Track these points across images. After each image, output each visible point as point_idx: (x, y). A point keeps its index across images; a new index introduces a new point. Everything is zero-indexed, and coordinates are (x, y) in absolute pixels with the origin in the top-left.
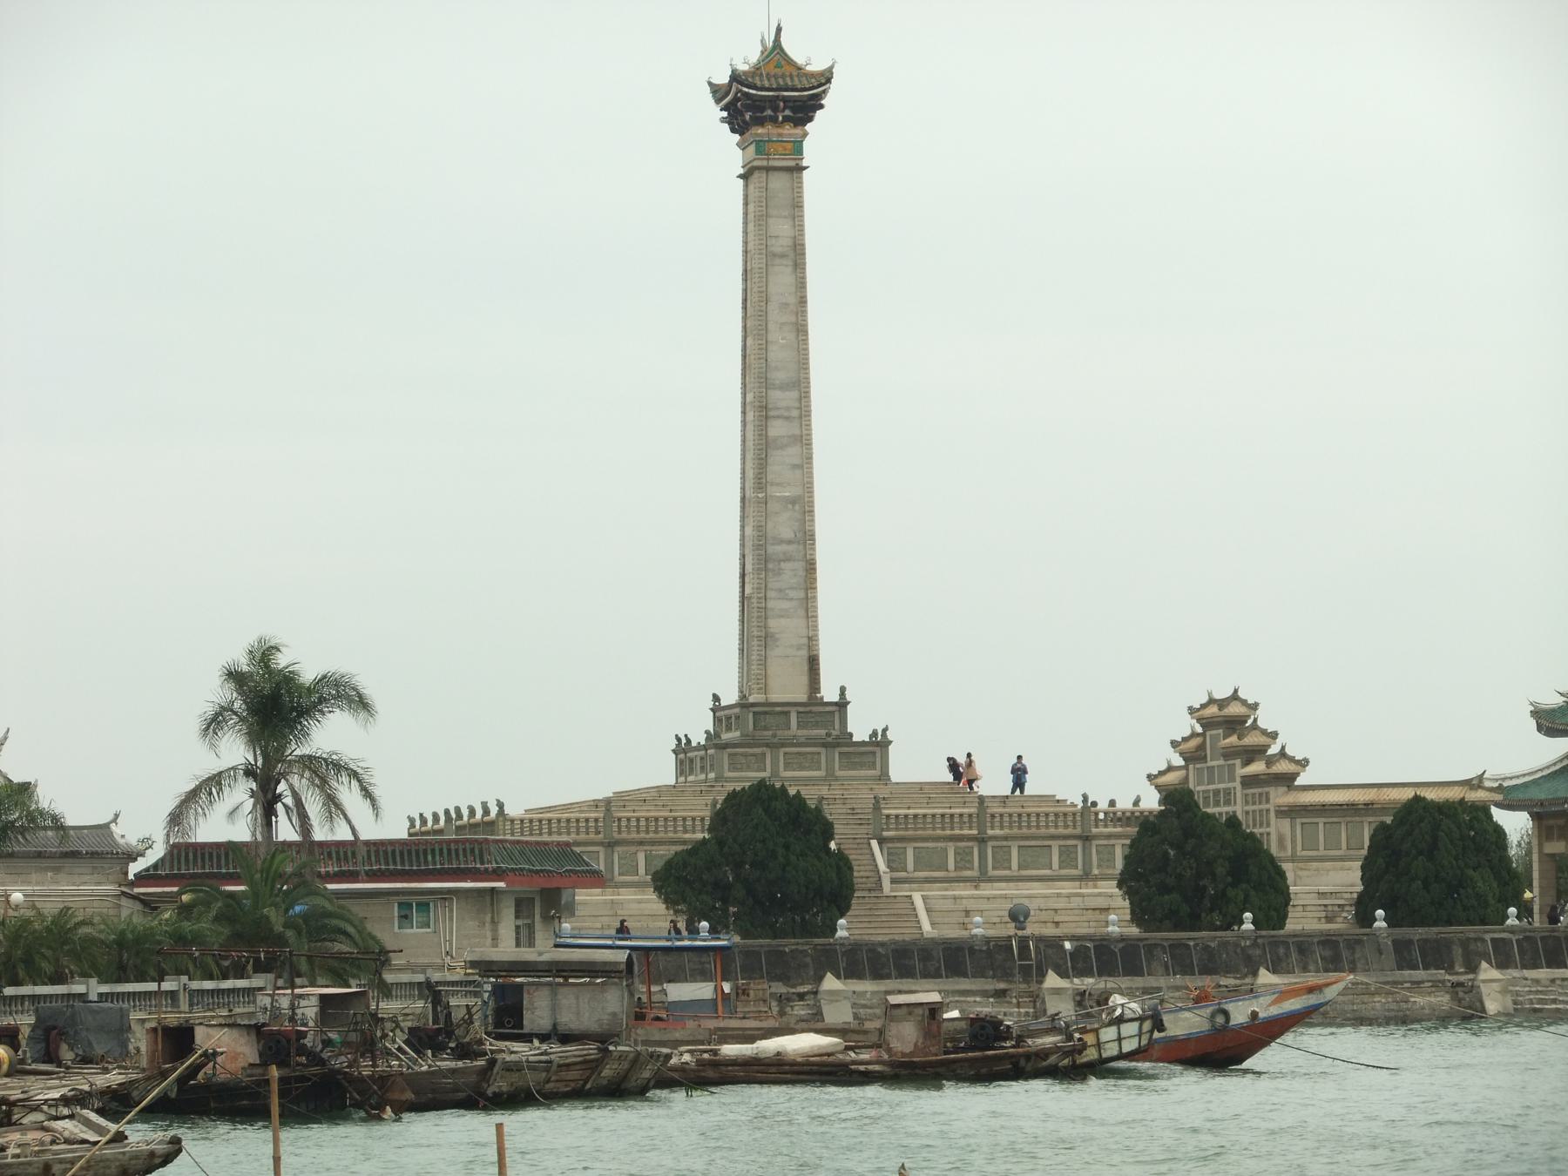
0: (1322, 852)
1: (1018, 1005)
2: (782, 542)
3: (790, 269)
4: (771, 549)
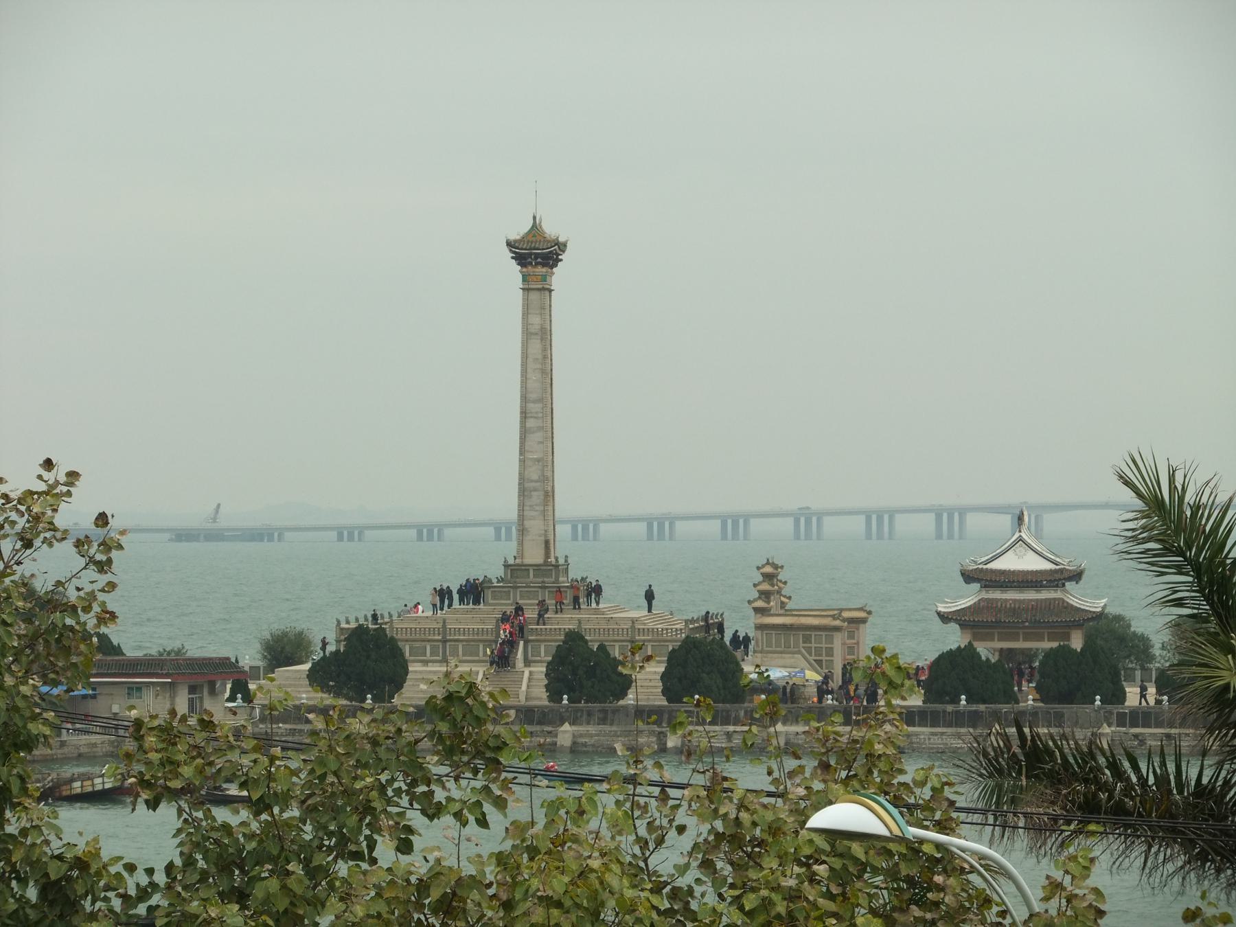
0: (774, 649)
4: (527, 485)
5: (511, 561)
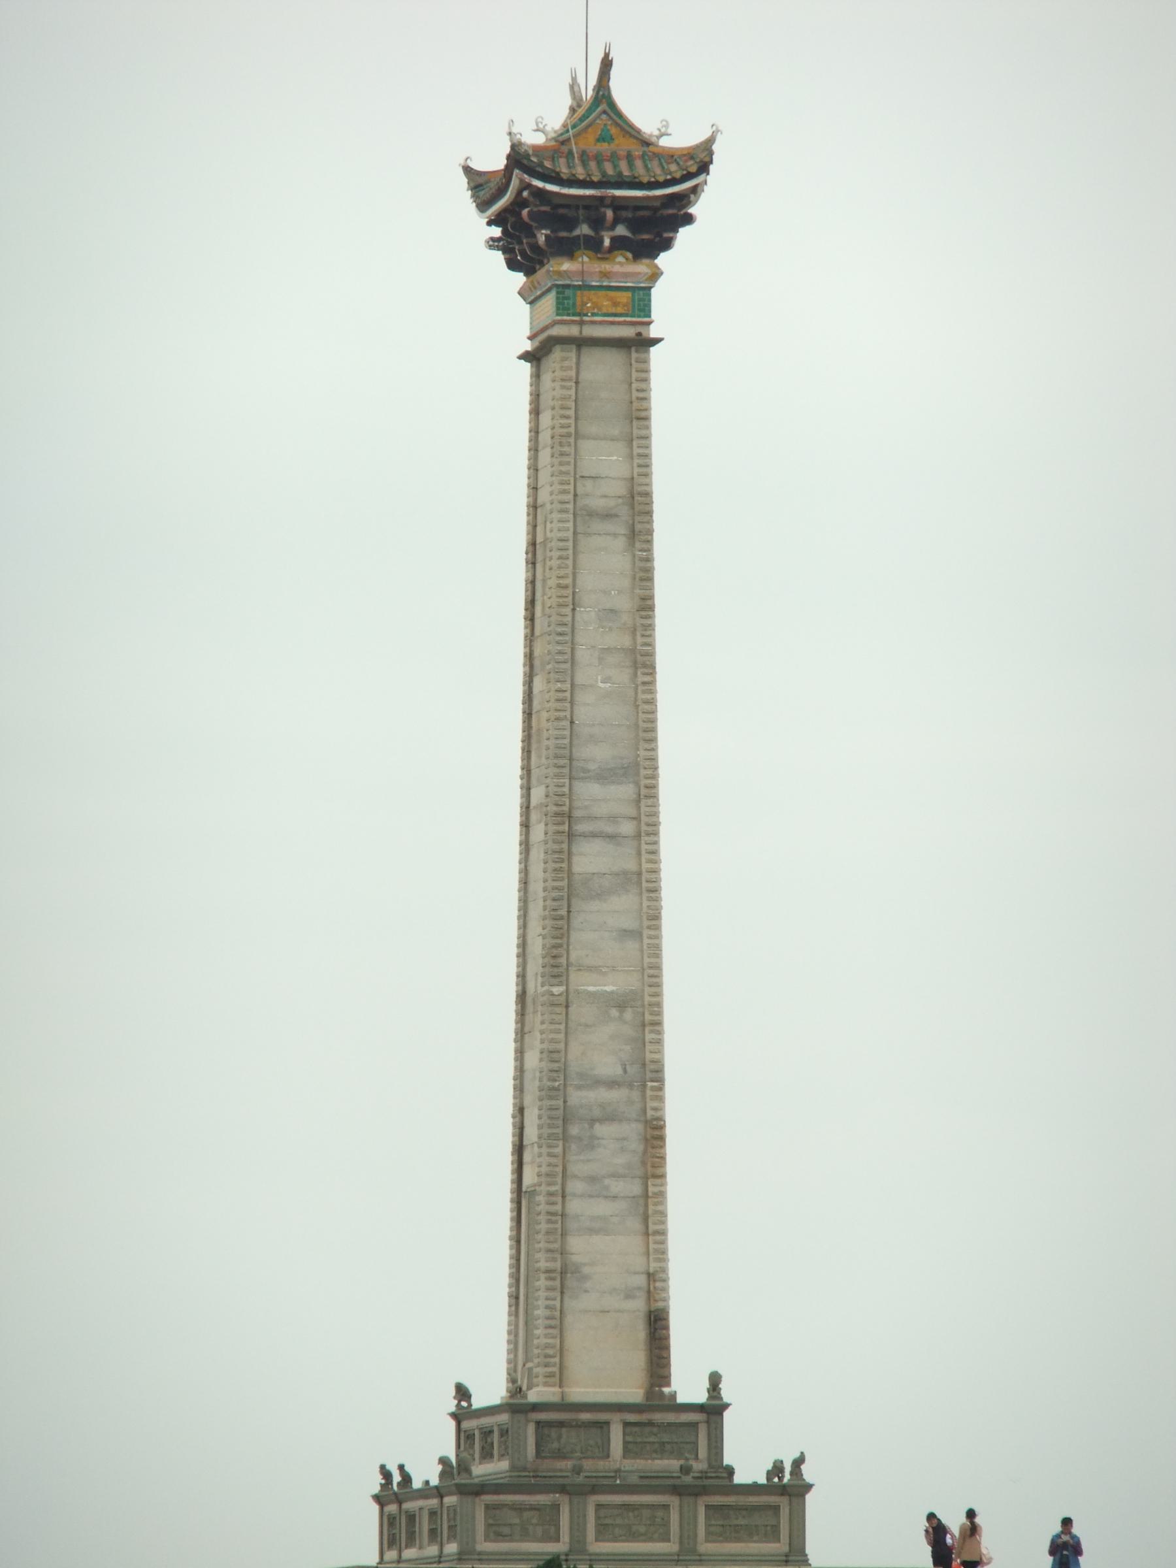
2: (598, 1082)
3: (620, 543)
4: (576, 1097)
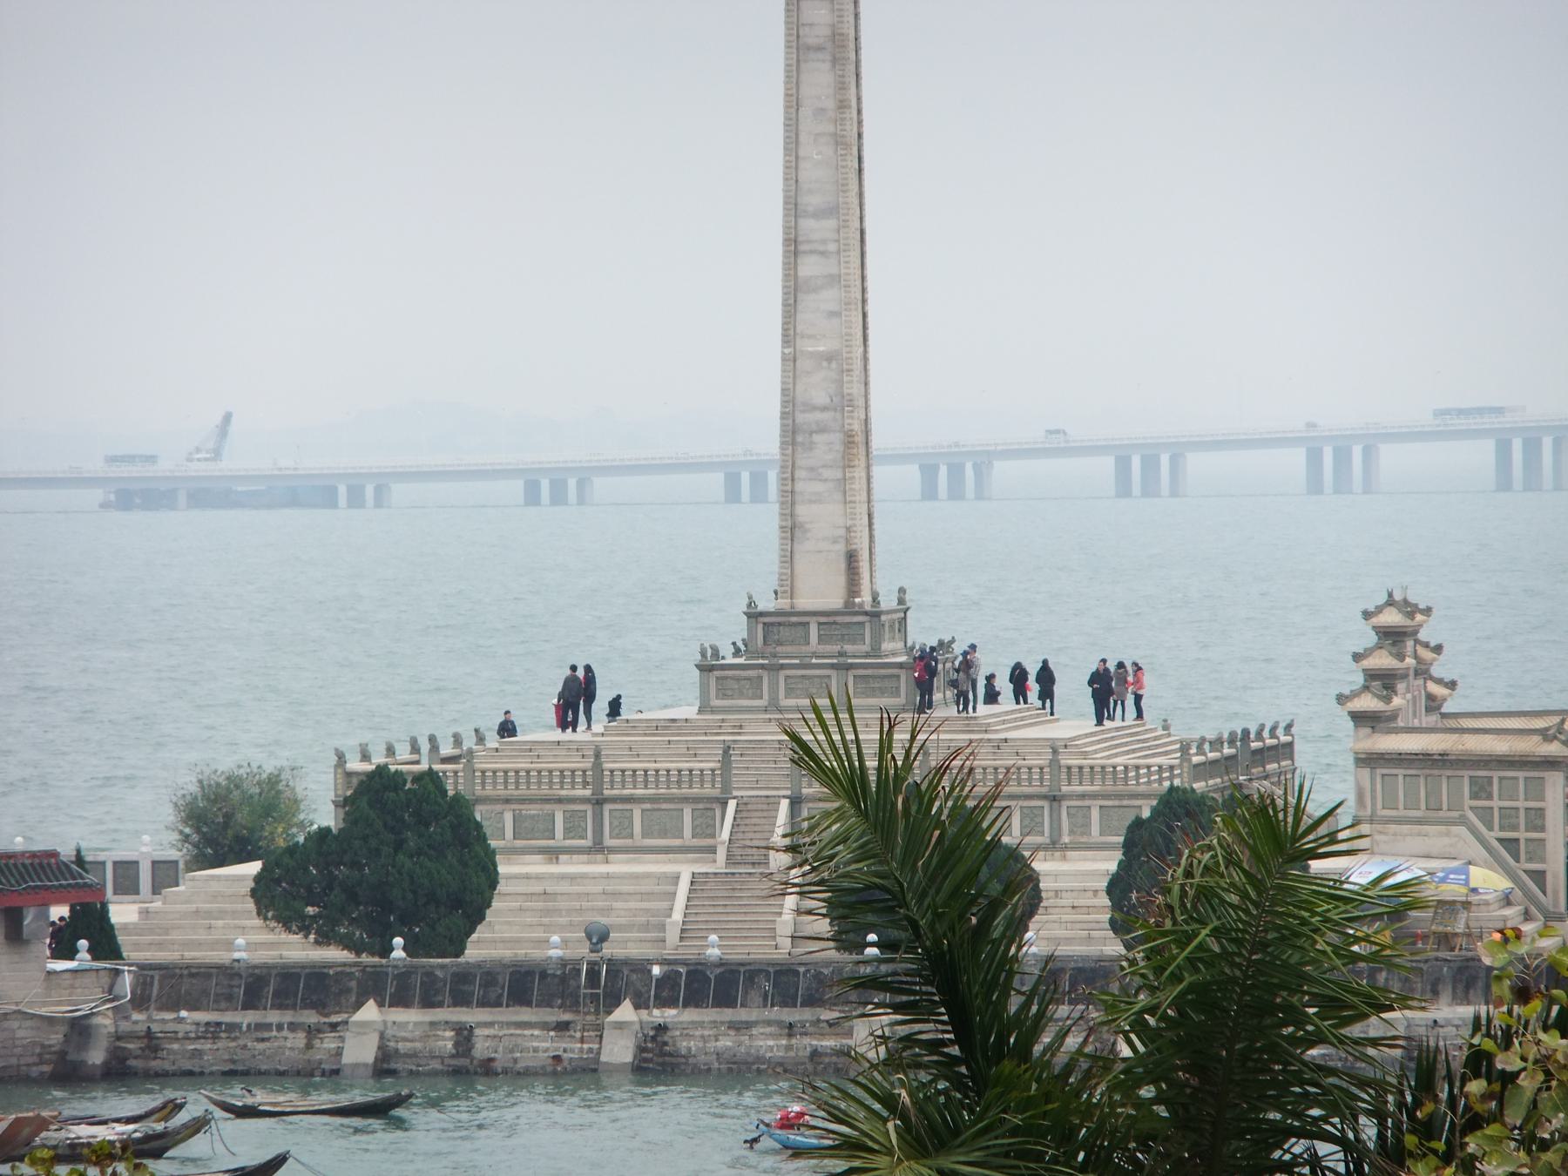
1: (582, 1041)
3: (827, 66)
5: (766, 603)
